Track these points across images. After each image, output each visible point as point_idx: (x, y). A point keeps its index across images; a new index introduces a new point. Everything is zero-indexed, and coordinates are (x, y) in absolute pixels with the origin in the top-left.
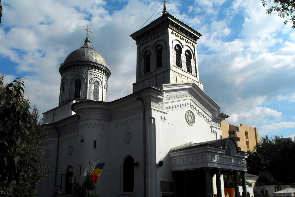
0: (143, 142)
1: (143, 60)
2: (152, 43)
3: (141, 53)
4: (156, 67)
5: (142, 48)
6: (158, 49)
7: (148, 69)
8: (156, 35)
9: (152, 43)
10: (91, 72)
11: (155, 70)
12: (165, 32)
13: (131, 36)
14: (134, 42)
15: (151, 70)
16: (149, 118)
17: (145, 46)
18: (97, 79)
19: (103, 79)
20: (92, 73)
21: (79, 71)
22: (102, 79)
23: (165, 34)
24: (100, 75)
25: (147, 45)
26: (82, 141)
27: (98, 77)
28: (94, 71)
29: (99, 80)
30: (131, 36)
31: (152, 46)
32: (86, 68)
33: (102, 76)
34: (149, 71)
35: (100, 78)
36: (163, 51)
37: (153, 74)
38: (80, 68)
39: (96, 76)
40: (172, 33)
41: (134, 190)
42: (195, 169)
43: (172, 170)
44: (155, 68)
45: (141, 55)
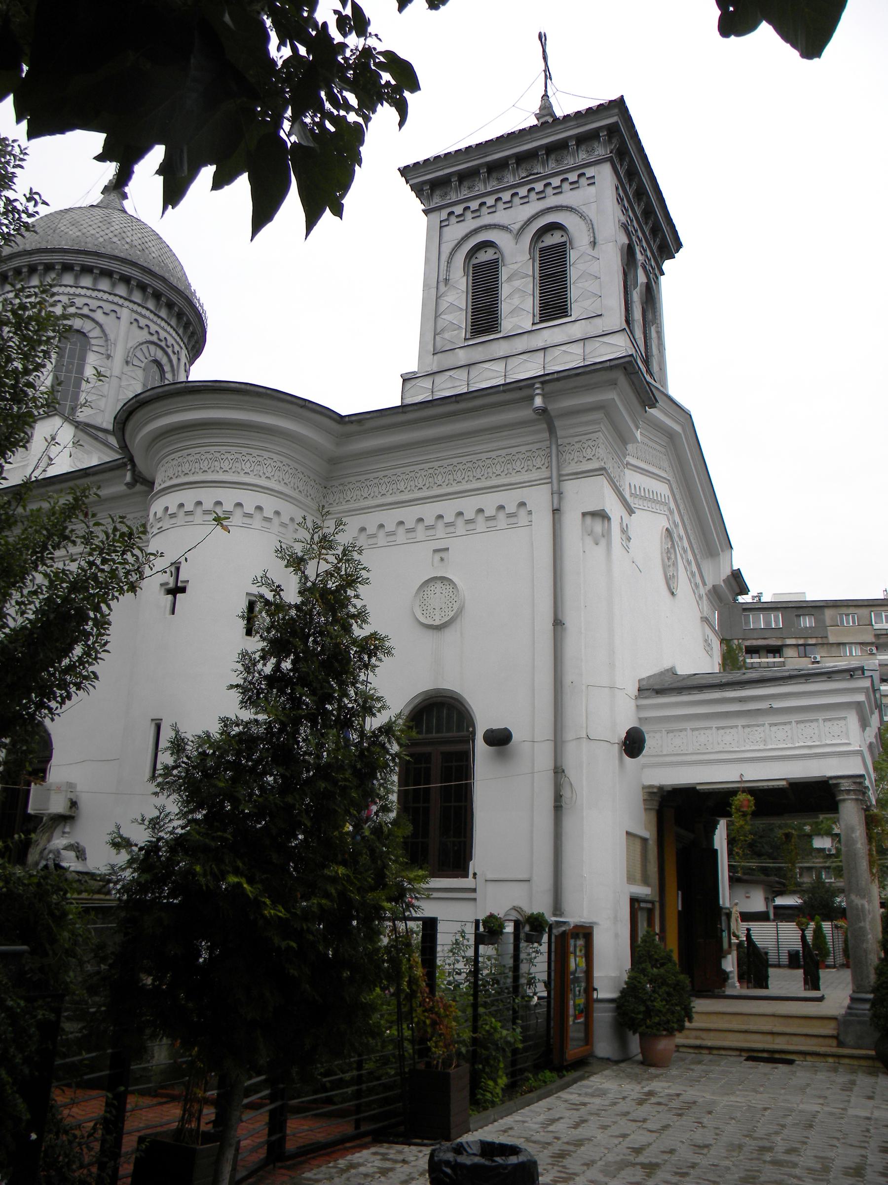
0: (551, 627)
1: (461, 282)
3: (447, 249)
4: (534, 316)
5: (456, 231)
6: (544, 245)
7: (484, 319)
8: (539, 186)
9: (520, 213)
10: (136, 312)
11: (529, 327)
12: (588, 175)
13: (405, 172)
15: (508, 325)
16: (584, 514)
17: (470, 224)
18: (159, 355)
19: (179, 359)
20: (143, 322)
21: (85, 296)
22: (174, 358)
24: (170, 341)
26: (176, 590)
27: (163, 344)
28: (152, 316)
29: (164, 361)
30: (405, 172)
31: (517, 227)
32: (117, 292)
33: (177, 348)
35: (169, 351)
36: (573, 255)
37: (520, 344)
38: (89, 285)
39: (154, 338)
41: (474, 866)
42: (784, 783)
43: (648, 782)
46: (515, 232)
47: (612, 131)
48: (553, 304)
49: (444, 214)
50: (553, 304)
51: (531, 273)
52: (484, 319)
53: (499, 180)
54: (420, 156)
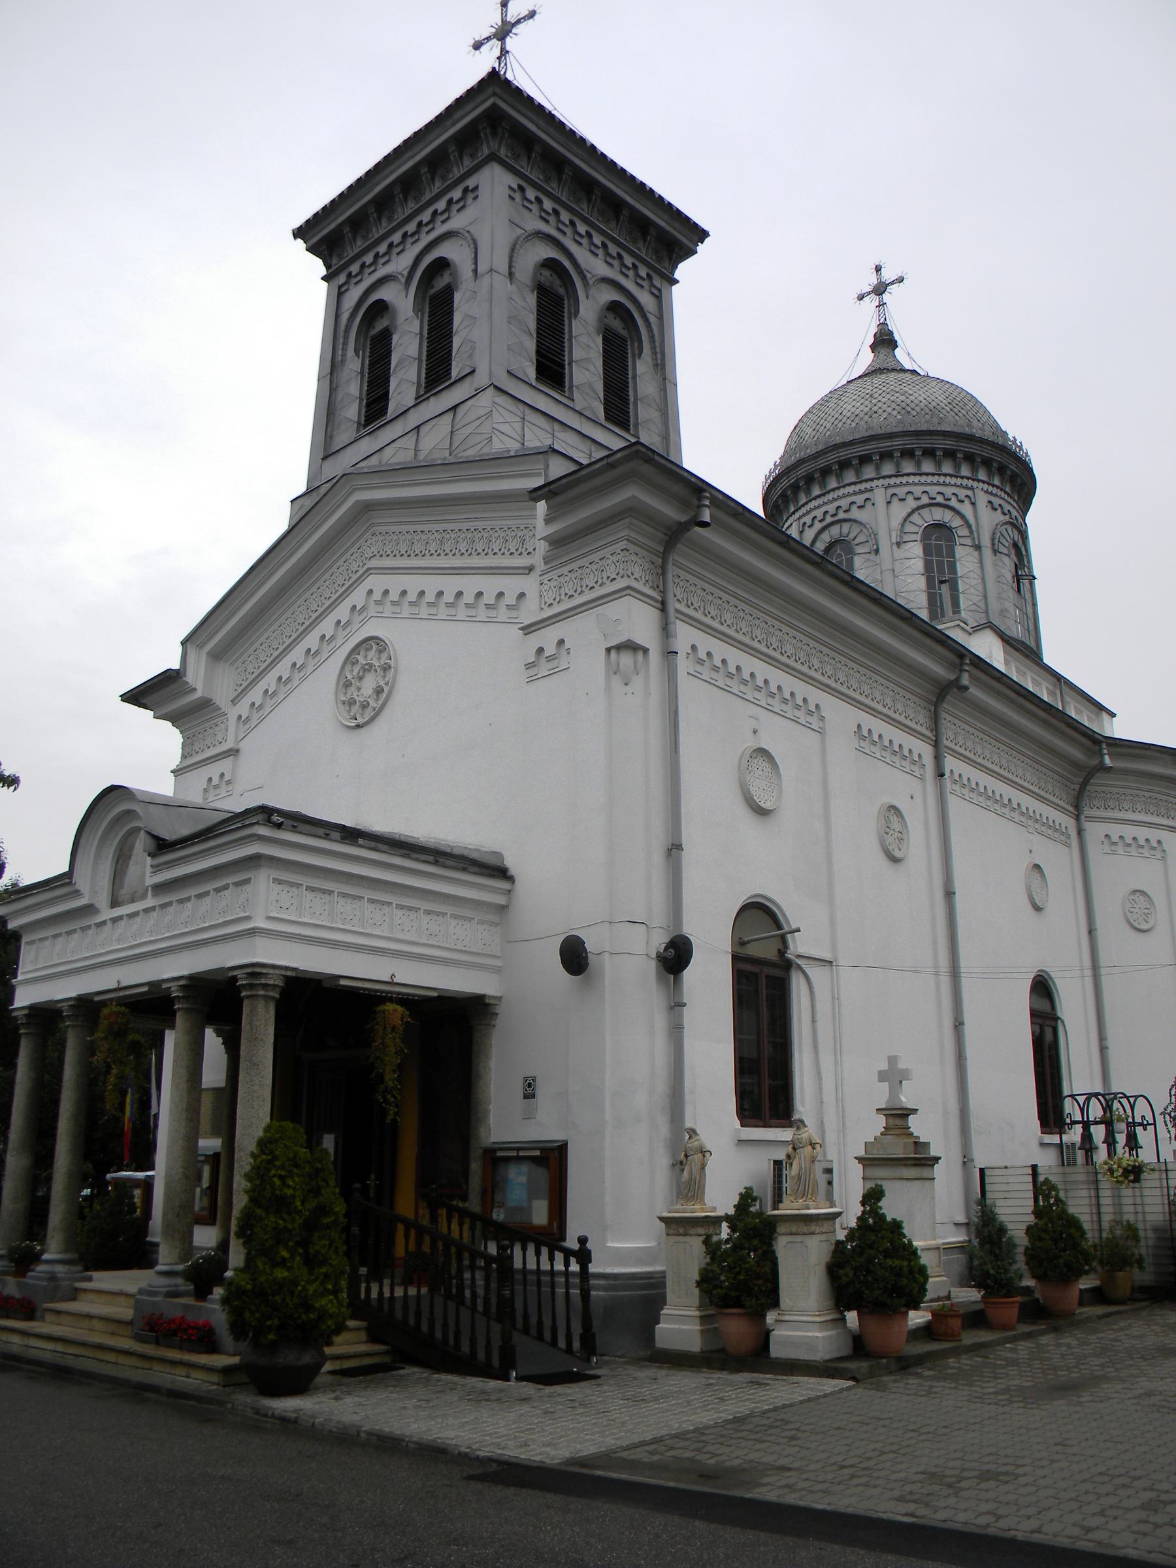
1: (354, 365)
2: (401, 263)
6: (432, 291)
7: (376, 407)
13: (299, 233)
14: (318, 267)
15: (393, 408)
23: (475, 198)
25: (382, 272)
30: (299, 233)
31: (405, 273)
34: (384, 410)
36: (457, 297)
40: (518, 196)
44: (414, 395)
45: (346, 337)
46: (403, 280)
47: (494, 120)
48: (437, 370)
49: (342, 278)
50: (437, 370)
51: (418, 331)
52: (376, 407)
53: (390, 219)
54: (308, 214)
